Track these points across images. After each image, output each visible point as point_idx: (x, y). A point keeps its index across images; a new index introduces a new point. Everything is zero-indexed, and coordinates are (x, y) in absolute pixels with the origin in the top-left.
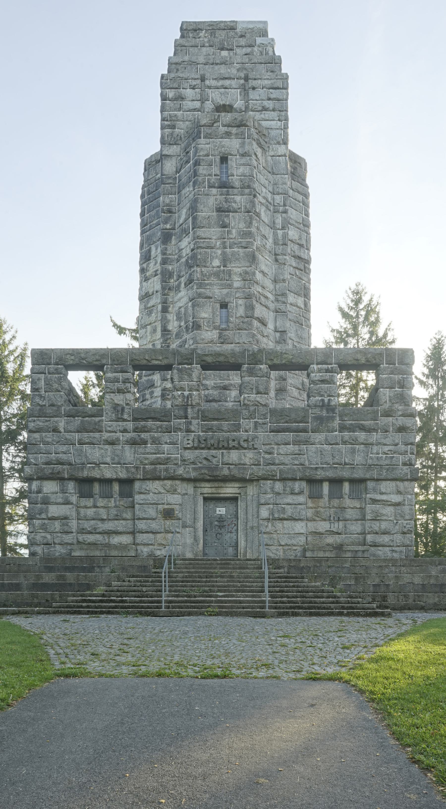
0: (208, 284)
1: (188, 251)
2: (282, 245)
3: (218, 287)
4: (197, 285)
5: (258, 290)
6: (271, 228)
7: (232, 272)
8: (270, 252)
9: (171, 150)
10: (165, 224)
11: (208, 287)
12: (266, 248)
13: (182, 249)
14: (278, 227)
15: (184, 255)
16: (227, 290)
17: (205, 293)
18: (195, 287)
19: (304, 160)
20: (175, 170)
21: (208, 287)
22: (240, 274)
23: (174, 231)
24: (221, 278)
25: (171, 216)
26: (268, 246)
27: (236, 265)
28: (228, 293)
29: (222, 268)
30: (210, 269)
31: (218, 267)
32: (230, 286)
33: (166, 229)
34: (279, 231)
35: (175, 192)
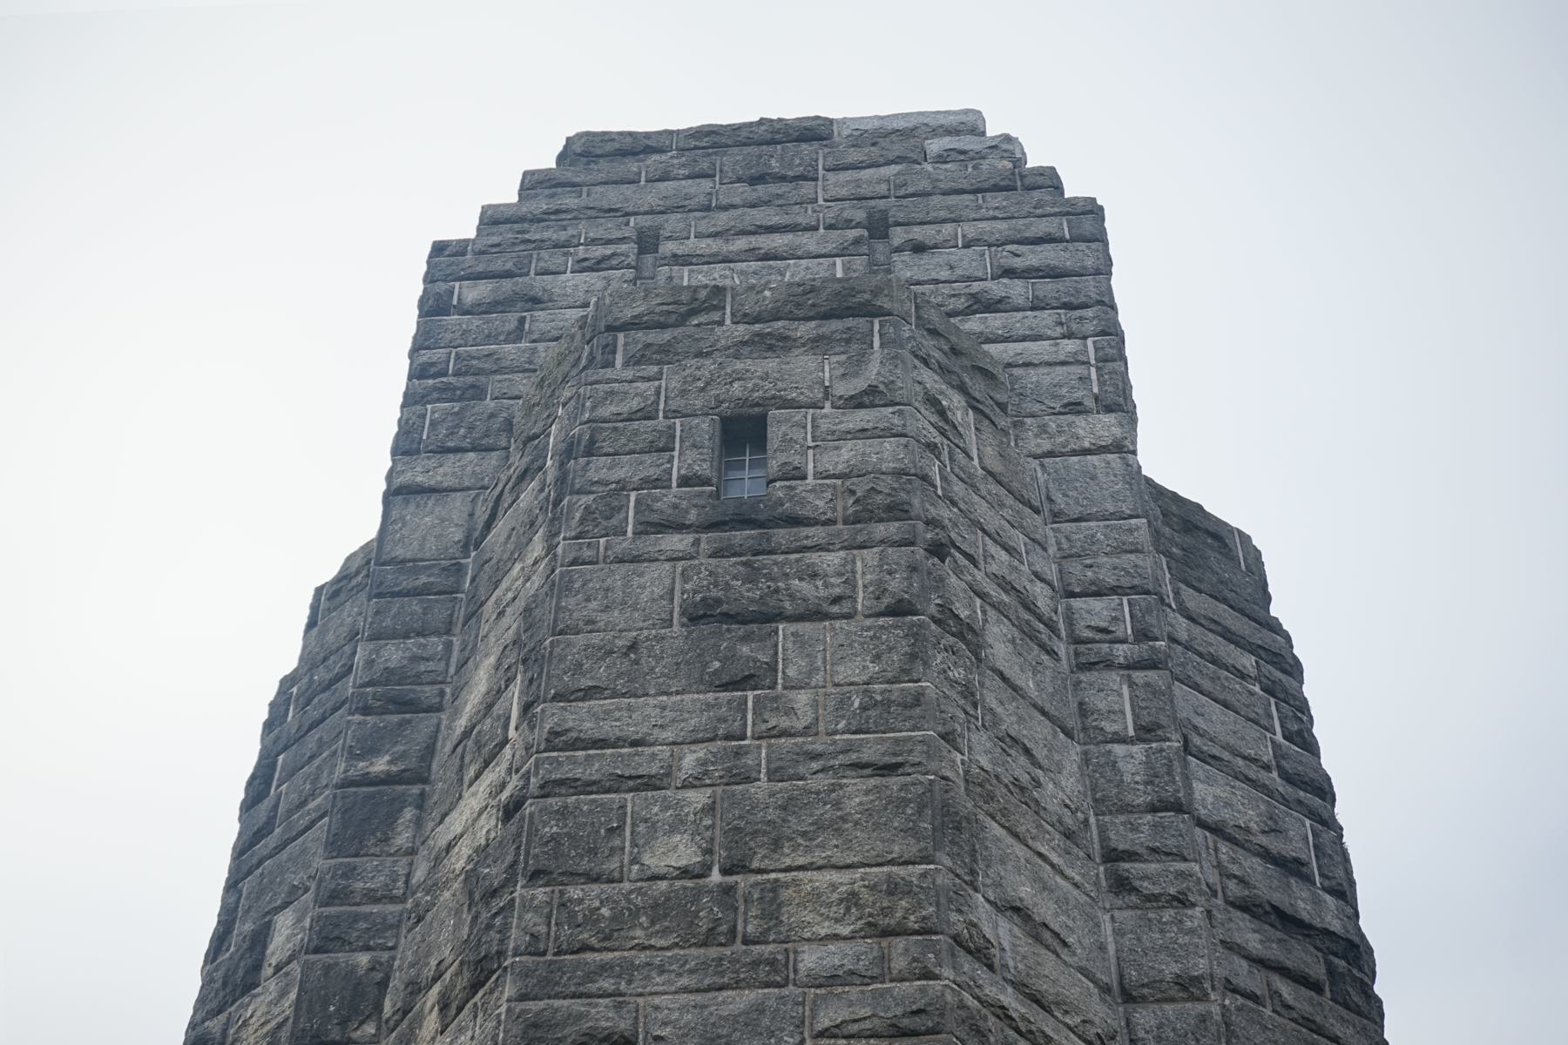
0: (604, 968)
1: (488, 825)
2: (1153, 809)
3: (684, 981)
4: (526, 974)
5: (990, 991)
6: (1068, 734)
7: (785, 894)
8: (1068, 835)
9: (446, 469)
10: (361, 757)
11: (607, 984)
12: (1038, 808)
13: (449, 847)
14: (1110, 728)
15: (461, 864)
16: (750, 996)
17: (581, 1016)
18: (509, 990)
19: (1245, 539)
20: (458, 535)
21: (607, 984)
22: (852, 899)
23: (415, 790)
24: (704, 925)
25: (401, 724)
26: (1053, 806)
27: (818, 857)
28: (759, 1009)
29: (716, 877)
30: (626, 886)
31: (685, 873)
32: (777, 973)
33: (367, 780)
34: (1119, 749)
35: (450, 623)
